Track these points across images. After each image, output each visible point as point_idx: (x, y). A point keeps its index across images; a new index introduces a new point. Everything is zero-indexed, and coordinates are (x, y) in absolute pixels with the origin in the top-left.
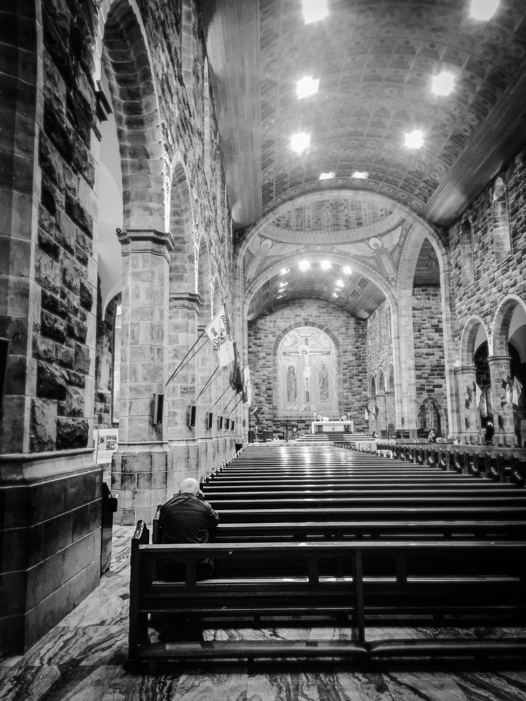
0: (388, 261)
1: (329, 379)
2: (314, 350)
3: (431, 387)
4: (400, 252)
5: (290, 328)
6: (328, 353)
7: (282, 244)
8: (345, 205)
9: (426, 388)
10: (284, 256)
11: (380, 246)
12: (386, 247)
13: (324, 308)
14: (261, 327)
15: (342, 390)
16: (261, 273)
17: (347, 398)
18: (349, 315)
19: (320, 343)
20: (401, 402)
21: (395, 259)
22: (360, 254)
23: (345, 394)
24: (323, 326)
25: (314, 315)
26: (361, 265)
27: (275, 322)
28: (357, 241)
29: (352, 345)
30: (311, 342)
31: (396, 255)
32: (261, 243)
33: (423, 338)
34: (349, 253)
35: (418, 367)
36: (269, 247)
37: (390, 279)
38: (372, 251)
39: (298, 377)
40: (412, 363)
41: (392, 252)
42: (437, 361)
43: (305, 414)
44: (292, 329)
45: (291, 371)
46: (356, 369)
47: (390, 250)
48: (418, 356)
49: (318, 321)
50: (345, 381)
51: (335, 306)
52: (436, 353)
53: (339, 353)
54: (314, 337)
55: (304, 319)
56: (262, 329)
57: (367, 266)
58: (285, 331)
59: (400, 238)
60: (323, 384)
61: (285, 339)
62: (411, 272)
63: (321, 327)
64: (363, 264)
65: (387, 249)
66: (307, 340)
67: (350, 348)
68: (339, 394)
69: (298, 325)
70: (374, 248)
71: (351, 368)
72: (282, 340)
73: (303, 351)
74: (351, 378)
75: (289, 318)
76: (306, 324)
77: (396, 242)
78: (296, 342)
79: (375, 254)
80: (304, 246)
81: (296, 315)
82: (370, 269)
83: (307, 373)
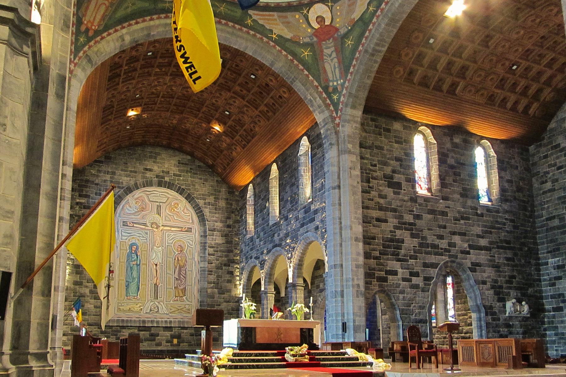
1: (188, 268)
2: (169, 223)
3: (383, 274)
4: (362, 35)
5: (137, 187)
6: (189, 230)
9: (377, 274)
11: (327, 23)
13: (186, 164)
14: (91, 179)
15: (206, 285)
17: (212, 296)
18: (220, 179)
19: (178, 214)
20: (342, 296)
22: (289, 36)
23: (209, 291)
24: (183, 190)
25: (172, 172)
27: (114, 173)
29: (221, 221)
30: (165, 211)
31: (349, 42)
33: (373, 193)
35: (368, 239)
38: (309, 30)
39: (143, 262)
40: (359, 229)
41: (346, 36)
42: (391, 232)
43: (151, 317)
44: (138, 188)
45: (133, 250)
46: (227, 256)
47: (343, 31)
48: (366, 221)
49: (178, 182)
50: (210, 273)
51: (202, 164)
52: (390, 220)
53: (205, 232)
54: (170, 203)
55: (157, 176)
56: (93, 182)
57: (296, 62)
58: (129, 190)
59: (369, 4)
60: (179, 274)
61: (128, 202)
63: (181, 191)
64: (290, 57)
65: (337, 30)
66: (159, 207)
67: (219, 225)
68: (201, 291)
69: (149, 184)
70: (316, 26)
71: (219, 254)
72: (123, 203)
73: (152, 224)
74: (218, 268)
75: (136, 172)
76: (160, 184)
77: (356, 15)
78: (143, 209)
81: (146, 169)
82: (301, 67)
83: (157, 256)
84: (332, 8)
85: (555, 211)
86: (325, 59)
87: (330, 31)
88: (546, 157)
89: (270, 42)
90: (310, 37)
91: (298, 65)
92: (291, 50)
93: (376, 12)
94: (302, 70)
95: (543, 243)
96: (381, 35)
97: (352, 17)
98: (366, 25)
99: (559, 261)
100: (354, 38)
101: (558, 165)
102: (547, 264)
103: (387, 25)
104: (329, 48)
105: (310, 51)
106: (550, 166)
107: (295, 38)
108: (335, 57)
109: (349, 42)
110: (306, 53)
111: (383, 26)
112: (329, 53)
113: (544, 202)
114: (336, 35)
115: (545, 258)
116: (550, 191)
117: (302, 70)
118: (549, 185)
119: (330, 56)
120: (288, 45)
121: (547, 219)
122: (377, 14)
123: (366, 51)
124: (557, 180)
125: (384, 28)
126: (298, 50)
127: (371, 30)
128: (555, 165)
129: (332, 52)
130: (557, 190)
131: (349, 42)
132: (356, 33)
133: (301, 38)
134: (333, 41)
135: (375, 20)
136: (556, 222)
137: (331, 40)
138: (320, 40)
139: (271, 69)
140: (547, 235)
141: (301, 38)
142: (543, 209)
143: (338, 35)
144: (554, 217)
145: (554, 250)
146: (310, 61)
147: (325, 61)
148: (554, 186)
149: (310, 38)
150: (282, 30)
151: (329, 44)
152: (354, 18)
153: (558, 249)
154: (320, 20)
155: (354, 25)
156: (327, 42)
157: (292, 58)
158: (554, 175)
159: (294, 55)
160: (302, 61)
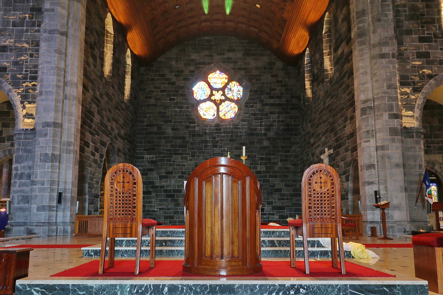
85: (155, 121)
88: (153, 80)
95: (141, 142)
99: (153, 157)
101: (162, 89)
102: (143, 158)
106: (155, 87)
113: (147, 112)
115: (142, 154)
116: (153, 105)
118: (152, 101)
121: (147, 125)
124: (159, 99)
128: (159, 88)
130: (159, 106)
136: (155, 129)
140: (146, 137)
142: (145, 117)
144: (153, 125)
145: (150, 149)
148: (157, 102)
153: (154, 149)
158: (157, 94)
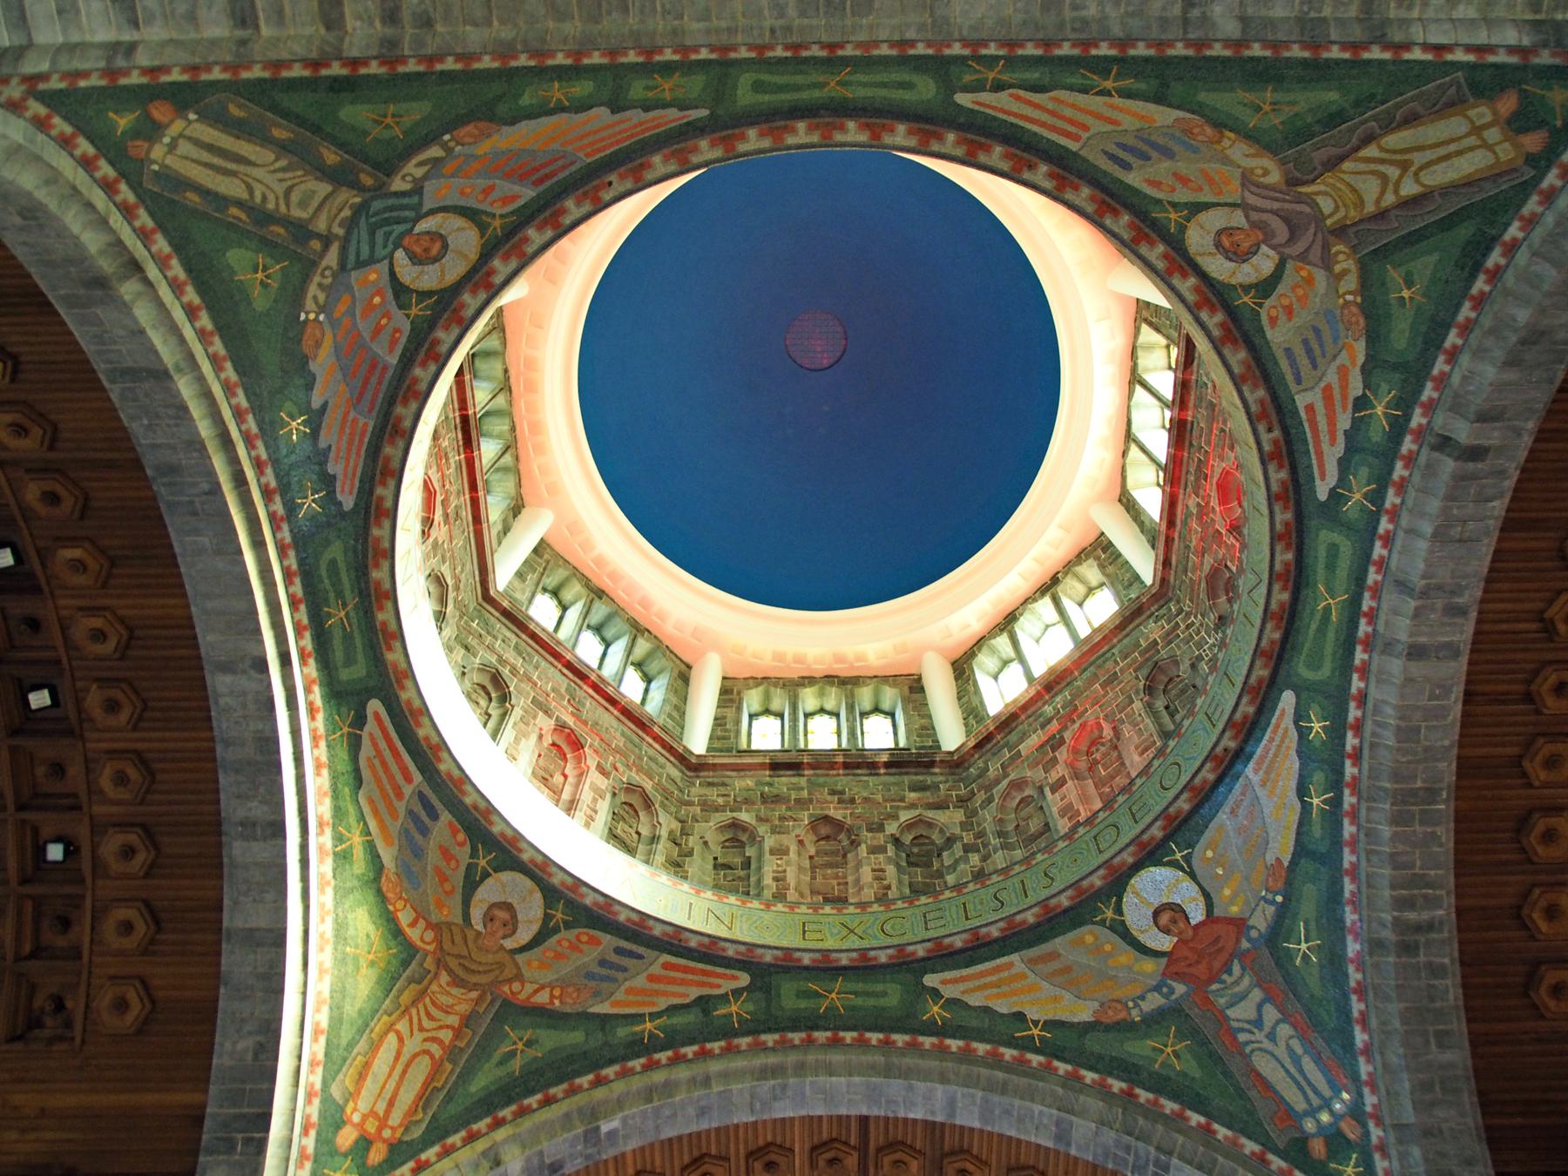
0: (1271, 1014)
7: (608, 940)
8: (968, 838)
10: (622, 1032)
11: (1197, 915)
12: (1234, 910)
16: (464, 1120)
21: (1313, 982)
26: (1103, 1091)
28: (1054, 922)
31: (1302, 946)
32: (472, 883)
34: (1020, 1017)
36: (524, 935)
37: (1318, 1148)
38: (1150, 966)
47: (1260, 921)
57: (1144, 1095)
59: (1302, 791)
62: (1443, 1039)
64: (1117, 1085)
65: (1240, 925)
70: (1165, 943)
79: (1180, 989)
80: (744, 979)
82: (1170, 1106)
84: (1190, 866)
86: (1247, 1043)
87: (1217, 939)
89: (1029, 1056)
90: (1157, 989)
91: (1156, 1103)
92: (1113, 1059)
93: (1336, 802)
94: (1180, 1116)
96: (1395, 861)
97: (1270, 858)
98: (1330, 859)
100: (1313, 925)
103: (1396, 820)
104: (1243, 997)
105: (1180, 1036)
107: (1110, 1013)
108: (1278, 1022)
109: (1304, 946)
110: (1169, 1050)
111: (1386, 831)
112: (1252, 1015)
114: (1245, 945)
117: (1180, 1116)
119: (1258, 1022)
120: (1093, 1044)
122: (1346, 806)
123: (1376, 946)
125: (1395, 837)
126: (1139, 1048)
127: (1355, 866)
129: (1260, 1007)
131: (1304, 946)
132: (1308, 906)
133: (1131, 1004)
134: (1243, 968)
135: (1348, 829)
137: (1236, 968)
138: (1200, 985)
139: (1068, 1155)
141: (1131, 1004)
143: (1250, 940)
146: (1195, 1071)
147: (1248, 1049)
149: (1160, 993)
150: (1056, 999)
151: (1236, 983)
152: (1278, 859)
154: (1169, 915)
155: (1289, 883)
156: (1224, 982)
157: (1124, 1085)
159: (1129, 1070)
160: (1162, 1084)
